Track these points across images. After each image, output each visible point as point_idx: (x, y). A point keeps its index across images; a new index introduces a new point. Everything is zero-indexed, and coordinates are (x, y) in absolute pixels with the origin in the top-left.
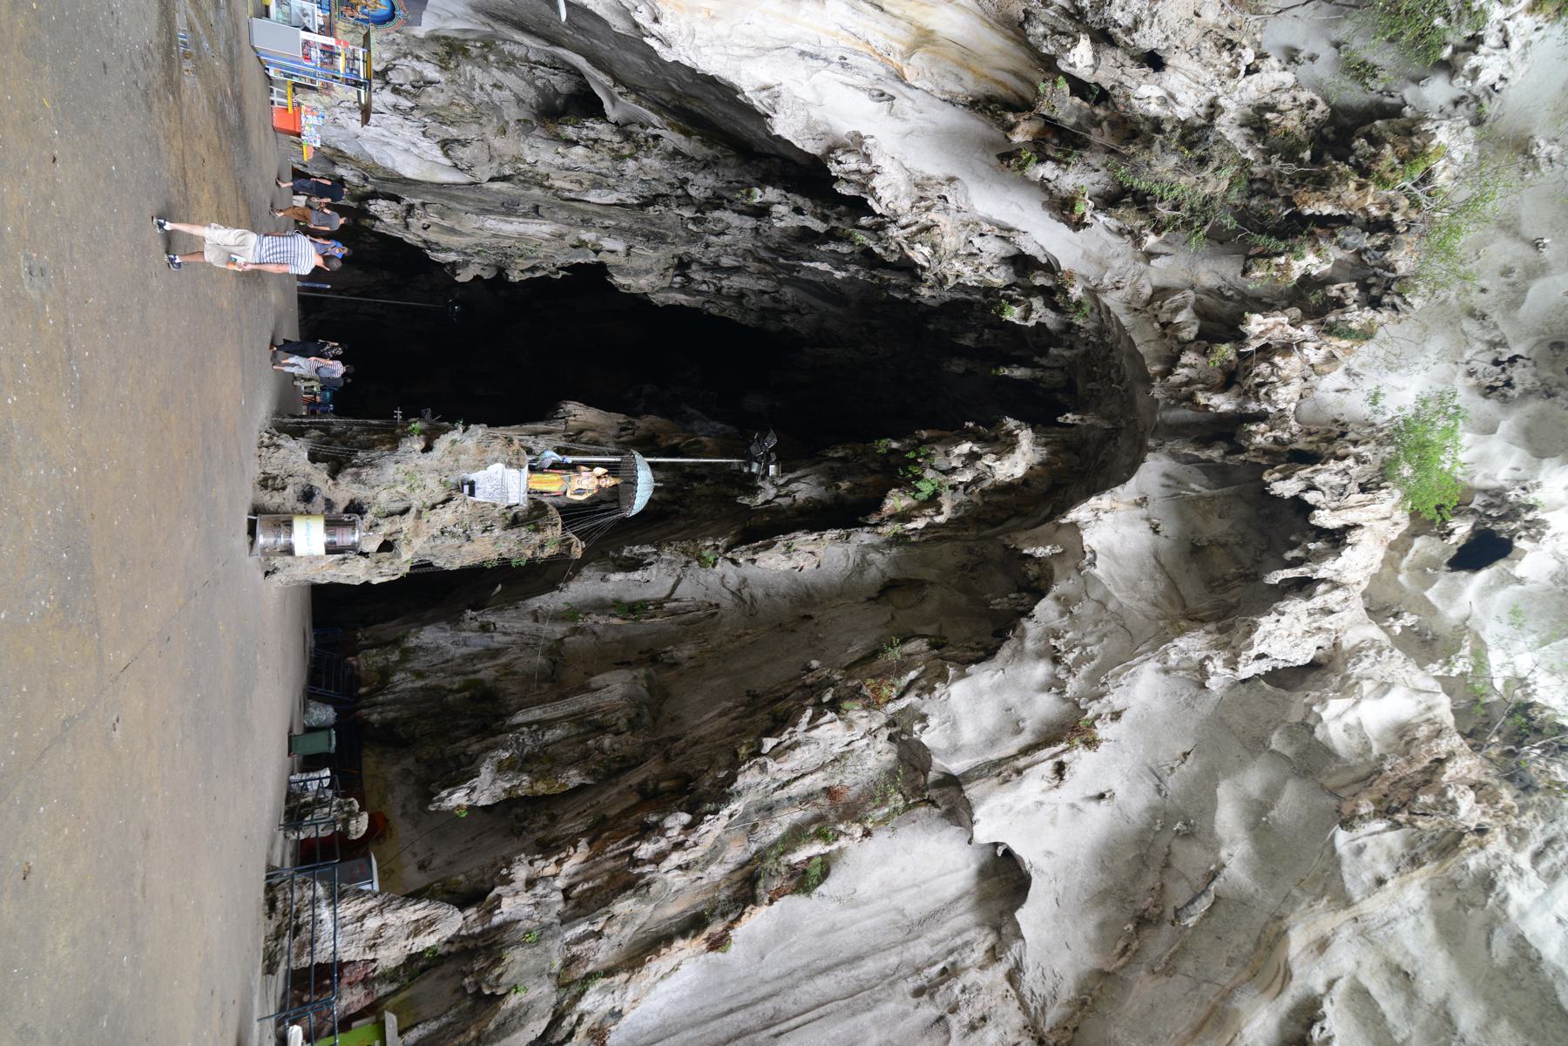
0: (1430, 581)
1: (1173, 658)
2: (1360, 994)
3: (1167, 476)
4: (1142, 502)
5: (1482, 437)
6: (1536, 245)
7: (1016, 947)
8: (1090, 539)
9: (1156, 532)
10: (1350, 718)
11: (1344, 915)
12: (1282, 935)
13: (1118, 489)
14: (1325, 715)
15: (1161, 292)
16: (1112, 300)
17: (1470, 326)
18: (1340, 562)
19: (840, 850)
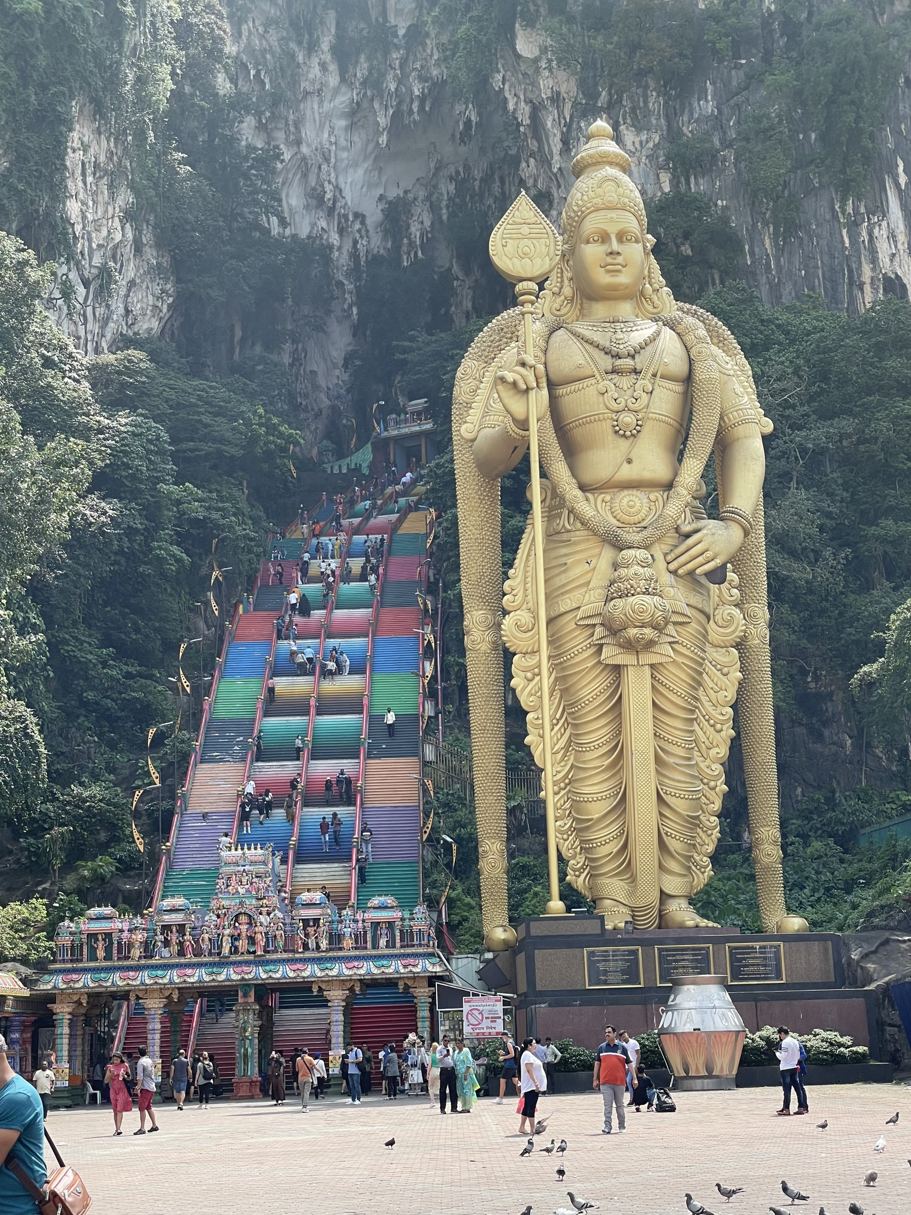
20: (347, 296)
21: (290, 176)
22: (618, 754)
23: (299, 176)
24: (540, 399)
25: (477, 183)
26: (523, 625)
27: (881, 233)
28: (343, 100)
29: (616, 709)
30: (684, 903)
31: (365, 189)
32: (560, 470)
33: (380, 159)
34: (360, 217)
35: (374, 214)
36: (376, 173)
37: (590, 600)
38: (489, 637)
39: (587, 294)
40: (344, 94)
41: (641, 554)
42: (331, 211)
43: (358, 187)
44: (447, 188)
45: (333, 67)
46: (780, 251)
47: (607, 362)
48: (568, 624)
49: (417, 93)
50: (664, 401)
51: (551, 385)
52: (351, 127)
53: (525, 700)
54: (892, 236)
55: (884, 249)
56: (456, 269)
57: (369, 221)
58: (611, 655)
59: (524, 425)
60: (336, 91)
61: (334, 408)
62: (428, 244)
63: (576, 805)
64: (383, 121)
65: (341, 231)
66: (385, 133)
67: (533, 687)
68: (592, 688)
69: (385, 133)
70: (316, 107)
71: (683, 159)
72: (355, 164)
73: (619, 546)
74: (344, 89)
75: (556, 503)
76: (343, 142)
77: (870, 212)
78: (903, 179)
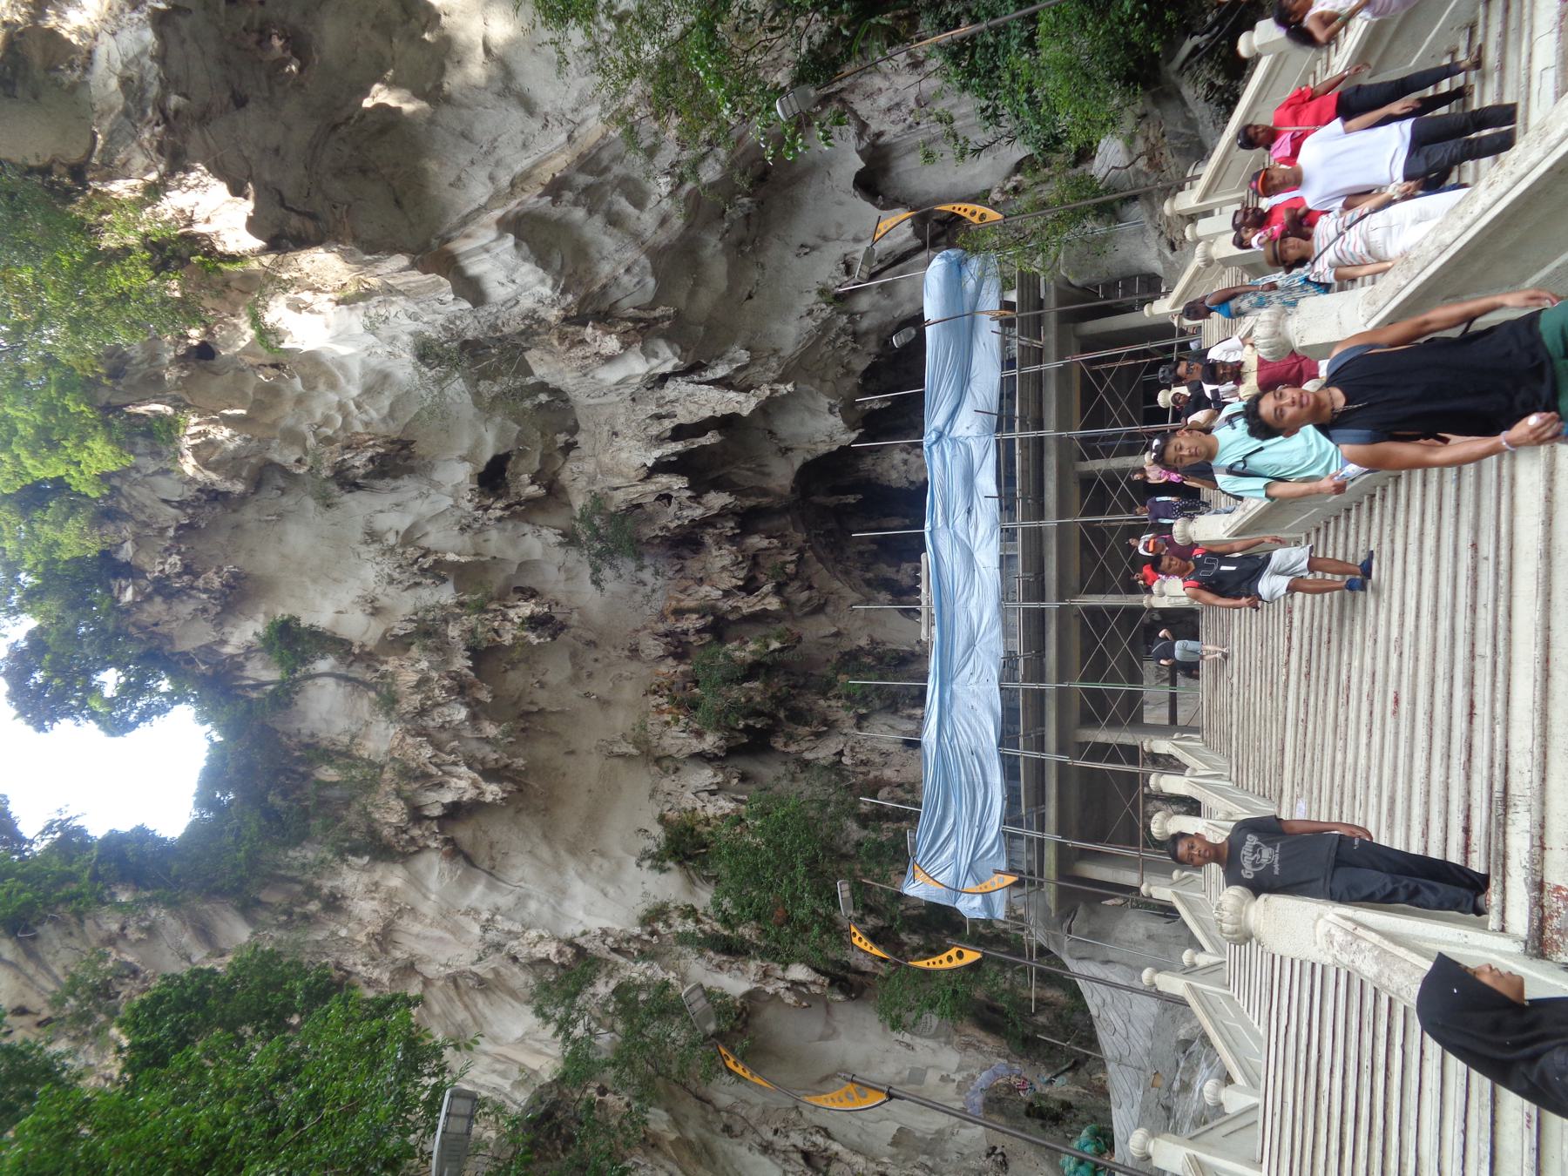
0: (519, 440)
1: (774, 363)
2: (639, 204)
3: (769, 475)
4: (785, 451)
5: (526, 558)
6: (587, 695)
7: (863, 144)
8: (835, 422)
9: (770, 432)
10: (654, 362)
11: (650, 243)
12: (687, 216)
13: (809, 458)
14: (676, 361)
15: (819, 609)
16: (855, 596)
17: (591, 636)
18: (657, 453)
19: (1008, 178)
20: (770, 990)
21: (461, 1015)
23: (480, 1000)
25: (682, 668)
28: (435, 869)
31: (611, 890)
35: (669, 886)
36: (598, 860)
40: (429, 867)
45: (380, 870)
49: (461, 713)
52: (494, 875)
56: (823, 752)
60: (416, 881)
65: (643, 955)
66: (484, 785)
69: (484, 785)
70: (417, 928)
72: (561, 892)
74: (421, 863)
76: (505, 901)
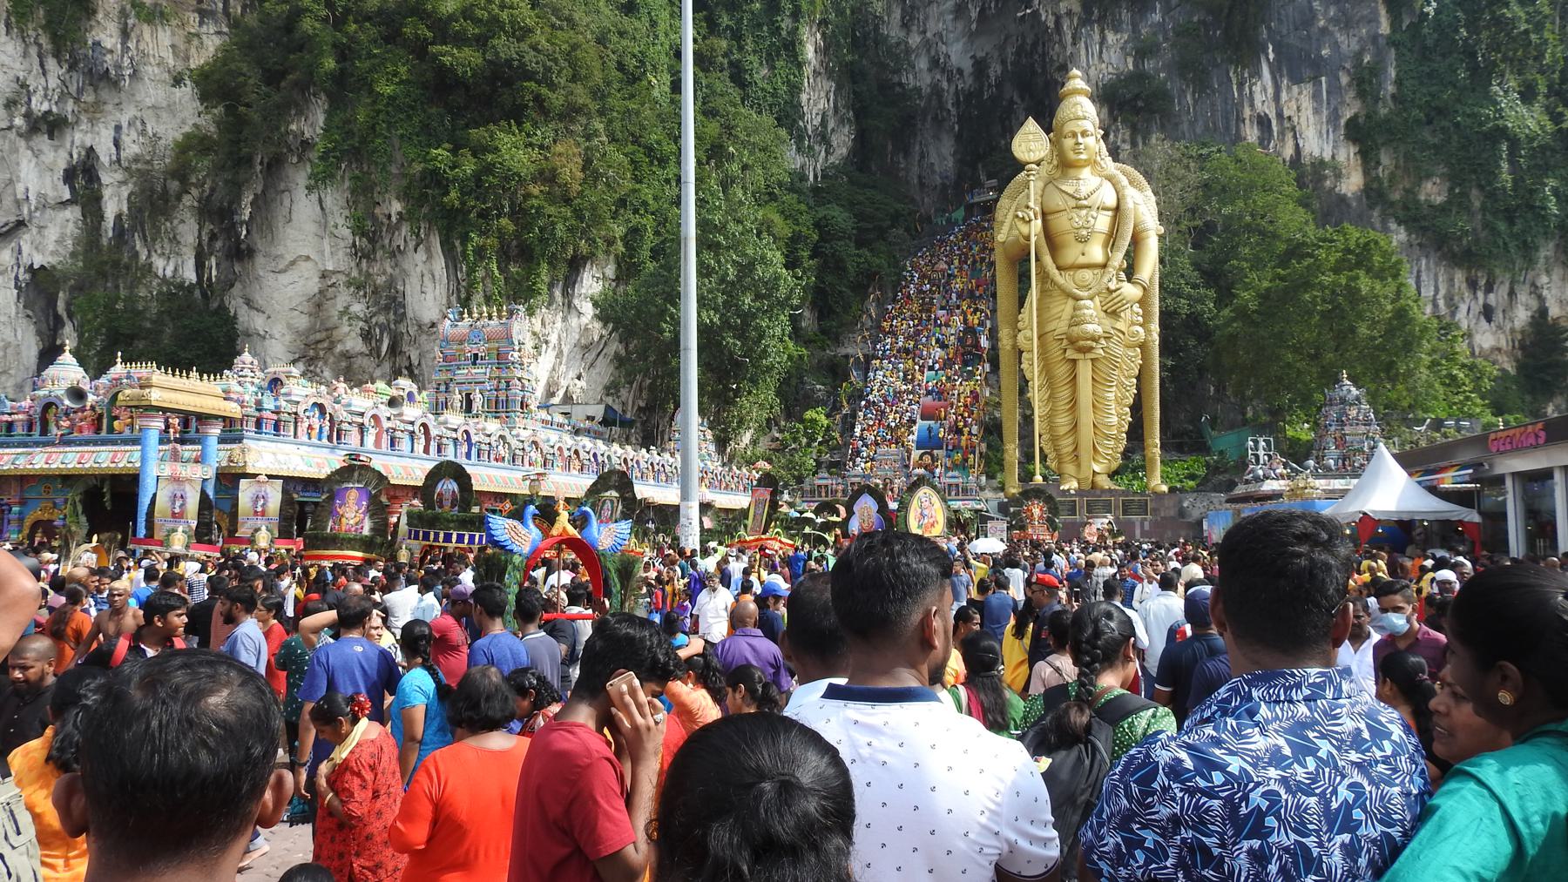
22: (1074, 403)
24: (1037, 225)
26: (1029, 335)
27: (1257, 89)
29: (1074, 380)
30: (1105, 477)
32: (1047, 259)
33: (972, 36)
34: (960, 72)
35: (967, 66)
37: (1060, 326)
38: (1010, 342)
39: (1065, 165)
41: (1088, 303)
42: (943, 70)
43: (958, 54)
44: (1010, 50)
46: (1196, 102)
47: (1072, 203)
48: (1050, 337)
50: (1103, 222)
51: (1044, 214)
52: (956, 19)
53: (1028, 376)
54: (1264, 89)
55: (1258, 98)
57: (966, 74)
58: (1071, 354)
59: (1028, 238)
61: (943, 184)
62: (999, 85)
63: (1052, 428)
64: (974, 14)
65: (949, 81)
67: (1033, 368)
68: (1062, 370)
71: (1142, 52)
72: (957, 40)
73: (1077, 299)
75: (1044, 276)
77: (1251, 76)
78: (1271, 56)
